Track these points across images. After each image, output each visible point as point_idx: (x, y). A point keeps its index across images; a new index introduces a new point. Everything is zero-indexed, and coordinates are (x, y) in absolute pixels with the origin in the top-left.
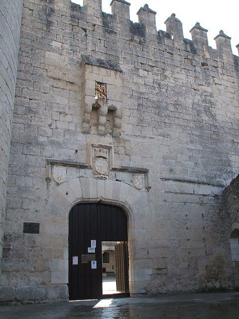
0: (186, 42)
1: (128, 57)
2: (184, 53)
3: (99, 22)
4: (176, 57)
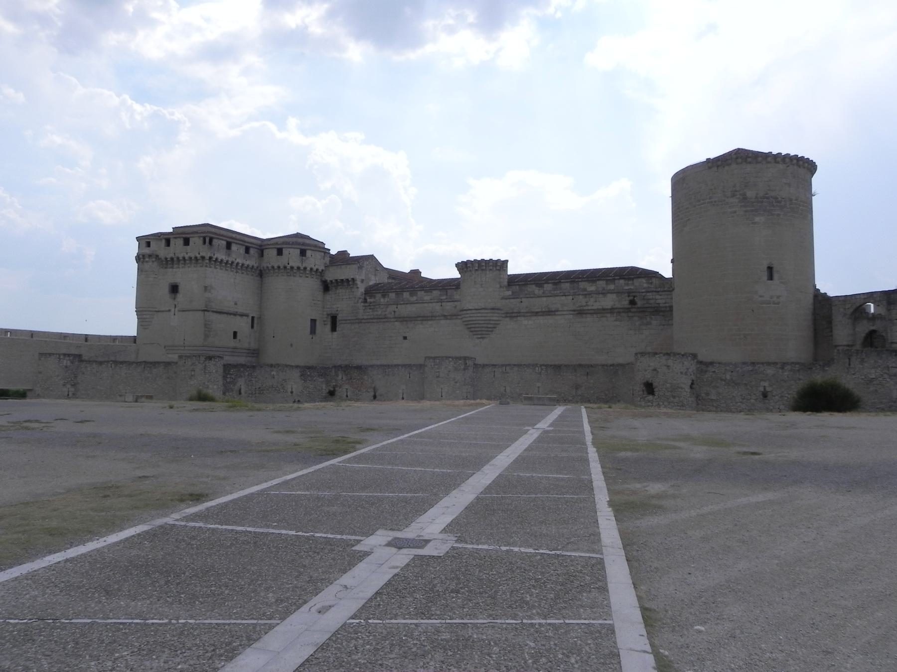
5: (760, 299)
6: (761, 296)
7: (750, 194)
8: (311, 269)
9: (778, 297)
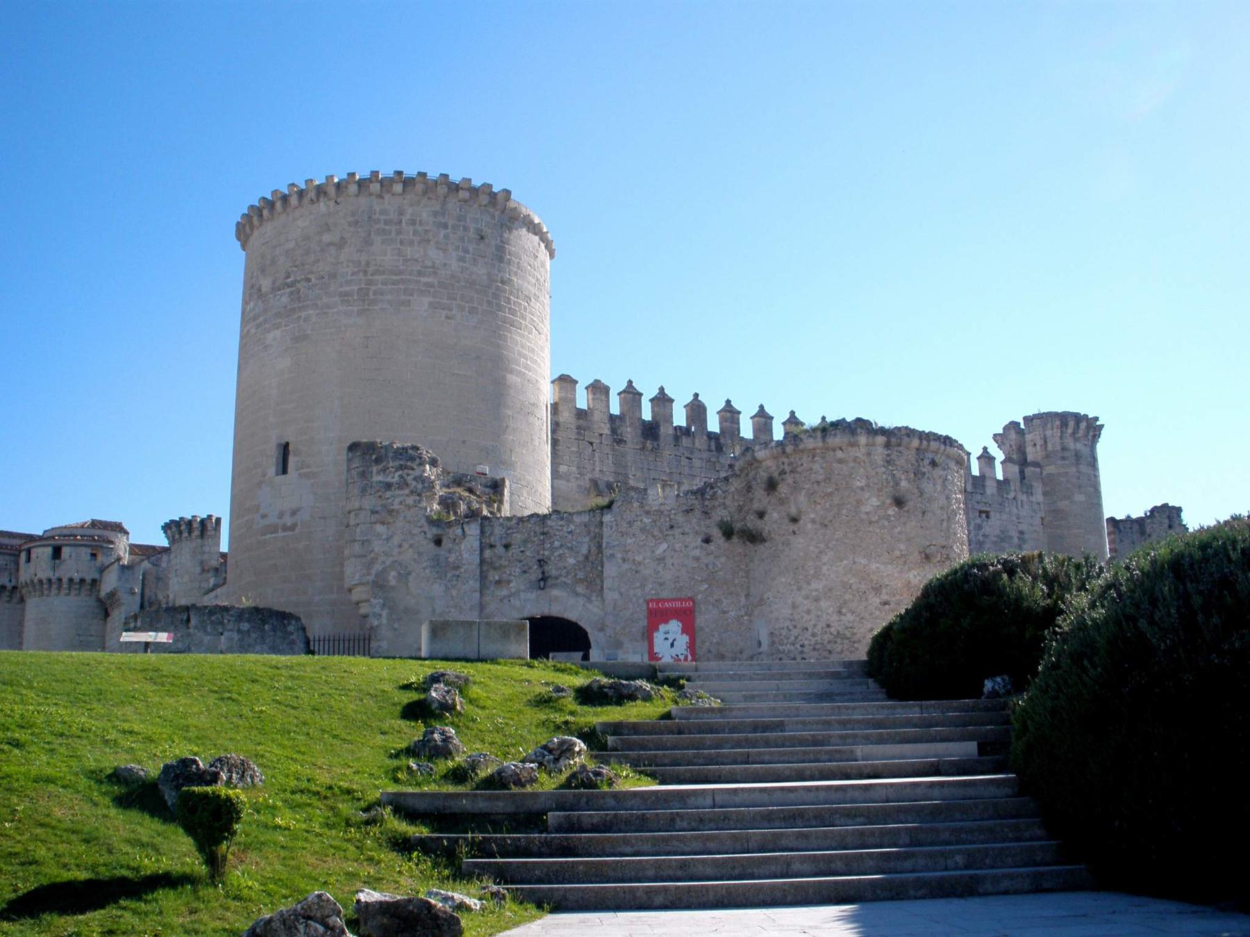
0: (711, 436)
1: (639, 474)
2: (705, 455)
3: (606, 430)
4: (697, 463)
5: (266, 522)
6: (264, 516)
7: (266, 284)
8: (71, 580)
9: (294, 513)
